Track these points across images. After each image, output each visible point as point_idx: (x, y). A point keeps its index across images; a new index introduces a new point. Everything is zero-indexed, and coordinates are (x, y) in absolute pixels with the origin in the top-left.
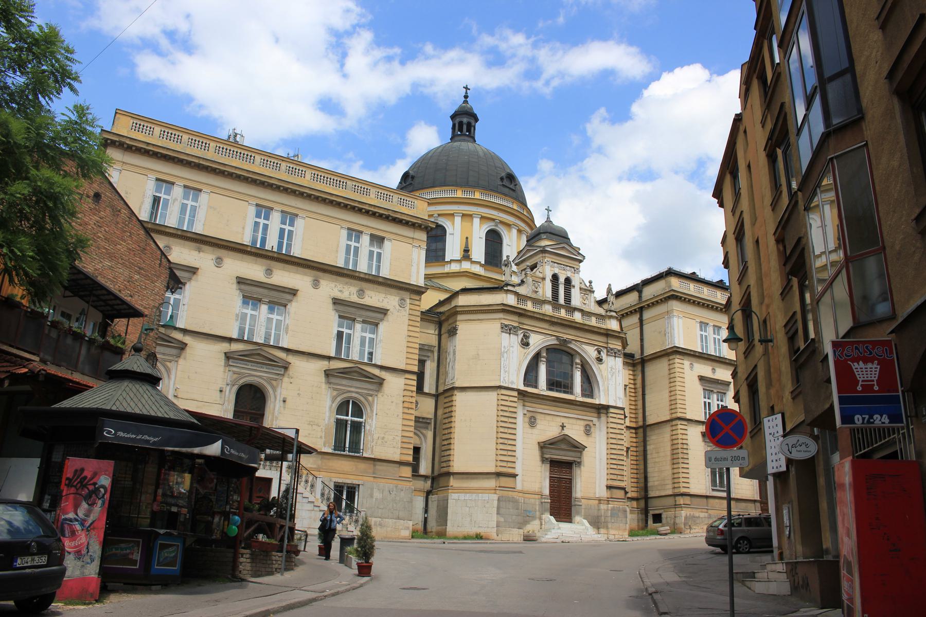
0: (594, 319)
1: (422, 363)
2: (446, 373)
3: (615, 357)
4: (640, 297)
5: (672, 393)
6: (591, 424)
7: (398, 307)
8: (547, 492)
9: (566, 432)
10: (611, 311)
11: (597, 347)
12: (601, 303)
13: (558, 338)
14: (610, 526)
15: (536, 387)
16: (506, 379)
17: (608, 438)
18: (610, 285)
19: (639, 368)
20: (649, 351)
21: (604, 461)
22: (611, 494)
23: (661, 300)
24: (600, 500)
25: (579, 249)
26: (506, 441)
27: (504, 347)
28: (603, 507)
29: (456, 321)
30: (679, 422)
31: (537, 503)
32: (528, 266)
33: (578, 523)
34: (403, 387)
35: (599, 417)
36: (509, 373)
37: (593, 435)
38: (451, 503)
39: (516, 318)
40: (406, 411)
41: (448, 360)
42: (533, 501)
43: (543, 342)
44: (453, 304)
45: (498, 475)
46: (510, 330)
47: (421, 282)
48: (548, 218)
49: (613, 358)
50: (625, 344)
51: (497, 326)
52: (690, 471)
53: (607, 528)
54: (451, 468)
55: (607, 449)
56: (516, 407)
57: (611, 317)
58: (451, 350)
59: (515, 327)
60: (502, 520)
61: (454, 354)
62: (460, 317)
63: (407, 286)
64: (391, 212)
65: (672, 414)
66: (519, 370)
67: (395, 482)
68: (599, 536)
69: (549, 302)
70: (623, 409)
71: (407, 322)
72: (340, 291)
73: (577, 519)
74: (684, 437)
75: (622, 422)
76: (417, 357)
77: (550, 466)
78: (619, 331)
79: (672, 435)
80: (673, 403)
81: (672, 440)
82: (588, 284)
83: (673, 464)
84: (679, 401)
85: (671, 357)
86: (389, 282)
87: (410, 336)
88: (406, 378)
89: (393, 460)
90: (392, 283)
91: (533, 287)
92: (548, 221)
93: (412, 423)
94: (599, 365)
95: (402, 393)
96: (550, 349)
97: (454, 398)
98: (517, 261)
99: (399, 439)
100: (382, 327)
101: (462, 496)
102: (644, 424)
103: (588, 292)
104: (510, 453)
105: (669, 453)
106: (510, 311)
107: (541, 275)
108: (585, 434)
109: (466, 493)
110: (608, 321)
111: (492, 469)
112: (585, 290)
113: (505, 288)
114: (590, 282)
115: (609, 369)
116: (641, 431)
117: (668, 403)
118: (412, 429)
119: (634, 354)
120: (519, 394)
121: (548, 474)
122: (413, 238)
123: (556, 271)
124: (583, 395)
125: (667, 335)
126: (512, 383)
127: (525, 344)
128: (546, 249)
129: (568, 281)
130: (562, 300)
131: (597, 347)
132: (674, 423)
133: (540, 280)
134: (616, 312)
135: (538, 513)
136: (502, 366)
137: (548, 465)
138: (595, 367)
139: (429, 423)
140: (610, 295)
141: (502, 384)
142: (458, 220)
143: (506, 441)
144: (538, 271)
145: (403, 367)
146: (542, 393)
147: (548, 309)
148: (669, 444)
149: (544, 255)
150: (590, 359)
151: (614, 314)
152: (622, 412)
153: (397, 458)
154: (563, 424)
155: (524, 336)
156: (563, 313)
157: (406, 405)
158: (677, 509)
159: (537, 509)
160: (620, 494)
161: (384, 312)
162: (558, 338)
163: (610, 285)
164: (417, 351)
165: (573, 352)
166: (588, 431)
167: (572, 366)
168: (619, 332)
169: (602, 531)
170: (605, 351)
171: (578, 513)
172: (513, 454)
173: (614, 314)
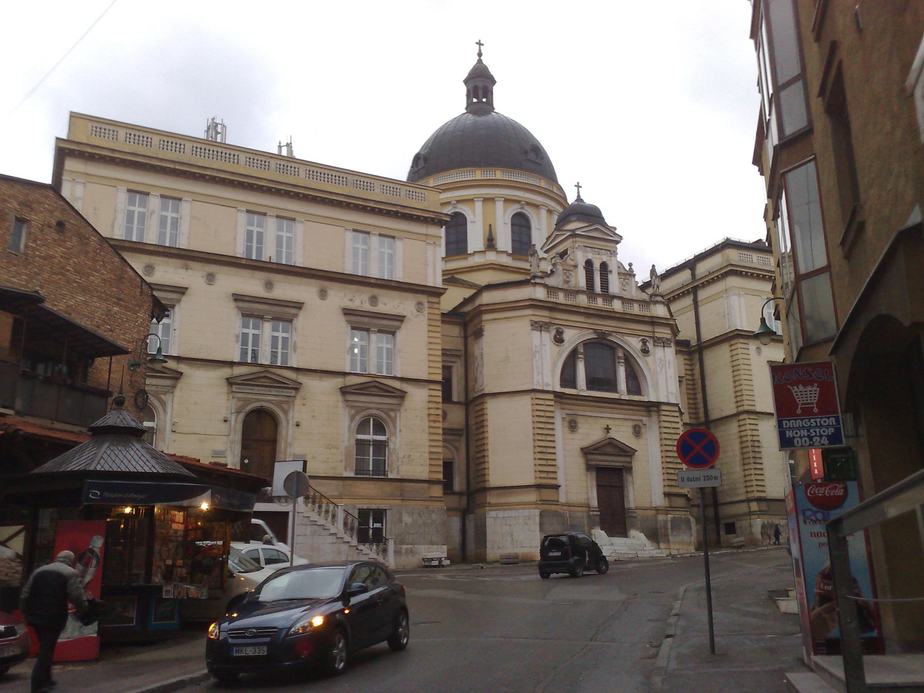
0: (636, 306)
1: (447, 369)
2: (476, 380)
3: (664, 347)
4: (693, 275)
5: (737, 383)
6: (640, 424)
7: (415, 312)
8: (594, 503)
9: (612, 434)
10: (656, 295)
11: (642, 338)
12: (645, 286)
13: (595, 331)
14: (671, 539)
15: (575, 387)
16: (540, 381)
17: (661, 439)
18: (653, 266)
19: (697, 356)
20: (706, 335)
21: (660, 466)
22: (670, 501)
23: (717, 276)
24: (657, 510)
25: (615, 228)
26: (544, 450)
27: (536, 347)
28: (661, 517)
29: (481, 322)
30: (745, 416)
32: (557, 254)
33: (634, 537)
34: (427, 399)
35: (650, 416)
36: (542, 374)
37: (644, 436)
38: (489, 522)
40: (432, 424)
41: (476, 365)
42: (580, 514)
43: (579, 337)
44: (478, 302)
45: (538, 487)
46: (541, 327)
47: (439, 283)
48: (579, 196)
50: (675, 331)
51: (526, 323)
52: (766, 472)
54: (487, 483)
55: (662, 451)
56: (553, 412)
57: (656, 302)
58: (477, 353)
59: (546, 323)
61: (482, 358)
62: (485, 317)
63: (424, 289)
64: (399, 207)
65: (738, 407)
66: (553, 370)
68: (660, 551)
69: (583, 292)
70: (677, 405)
71: (426, 327)
72: (351, 300)
73: (633, 533)
74: (754, 433)
75: (678, 420)
76: (440, 365)
77: (597, 474)
78: (669, 317)
79: (740, 432)
80: (738, 394)
81: (741, 437)
82: (627, 268)
83: (744, 464)
84: (745, 392)
85: (733, 342)
86: (404, 286)
87: (431, 343)
88: (430, 389)
90: (407, 286)
91: (565, 277)
92: (579, 199)
93: (440, 438)
94: (646, 358)
96: (587, 344)
97: (486, 406)
98: (545, 249)
99: (427, 455)
100: (400, 335)
101: (501, 514)
102: (705, 420)
103: (628, 277)
104: (550, 462)
105: (738, 452)
107: (572, 263)
109: (504, 510)
110: (652, 306)
111: (532, 481)
112: (625, 274)
113: (533, 281)
114: (630, 265)
115: (658, 362)
117: (734, 395)
118: (440, 444)
120: (555, 396)
121: (594, 483)
122: (426, 235)
123: (590, 256)
124: (629, 392)
125: (727, 316)
126: (548, 385)
127: (559, 340)
128: (577, 232)
129: (604, 266)
131: (642, 338)
132: (742, 417)
134: (662, 297)
136: (534, 367)
137: (594, 474)
138: (640, 360)
139: (460, 435)
140: (654, 277)
142: (479, 205)
143: (544, 450)
144: (569, 258)
146: (581, 393)
147: (582, 300)
148: (738, 441)
149: (574, 239)
150: (635, 352)
151: (660, 299)
152: (676, 409)
153: (425, 476)
154: (608, 426)
155: (557, 331)
156: (600, 303)
157: (432, 418)
158: (752, 517)
159: (586, 523)
160: (680, 502)
161: (400, 319)
162: (595, 331)
163: (653, 266)
165: (615, 346)
166: (637, 432)
168: (667, 319)
169: (662, 546)
170: (651, 341)
171: (633, 526)
172: (553, 463)
173: (660, 299)
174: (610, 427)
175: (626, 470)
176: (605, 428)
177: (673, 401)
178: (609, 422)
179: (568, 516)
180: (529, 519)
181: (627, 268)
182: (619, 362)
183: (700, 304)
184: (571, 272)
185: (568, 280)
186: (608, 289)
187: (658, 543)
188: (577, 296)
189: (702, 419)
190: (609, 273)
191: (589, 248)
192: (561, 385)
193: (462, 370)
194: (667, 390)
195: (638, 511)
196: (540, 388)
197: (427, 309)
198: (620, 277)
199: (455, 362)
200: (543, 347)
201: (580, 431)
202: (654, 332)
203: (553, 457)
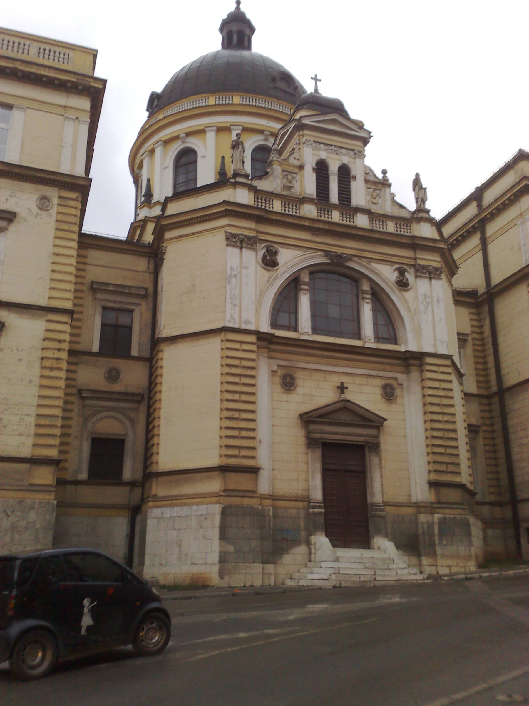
3: (430, 279)
4: (479, 206)
6: (394, 383)
7: (35, 210)
8: (317, 495)
9: (349, 396)
13: (327, 253)
14: (439, 550)
15: (296, 330)
17: (425, 405)
18: (417, 175)
19: (486, 308)
20: (497, 278)
21: (422, 441)
22: (438, 494)
24: (418, 507)
26: (236, 415)
27: (232, 269)
28: (423, 518)
31: (302, 516)
34: (42, 334)
35: (408, 372)
37: (399, 400)
39: (252, 225)
40: (47, 373)
42: (294, 512)
43: (301, 261)
49: (427, 281)
51: (221, 237)
53: (434, 555)
56: (253, 360)
59: (249, 238)
60: (230, 548)
64: (18, 63)
66: (259, 303)
67: (20, 495)
70: (449, 357)
71: (52, 233)
86: (16, 170)
87: (58, 255)
88: (48, 321)
89: (18, 456)
90: (23, 172)
91: (285, 181)
94: (404, 293)
95: (40, 344)
99: (32, 420)
101: (168, 512)
103: (380, 187)
106: (240, 213)
107: (297, 163)
108: (384, 400)
111: (214, 461)
114: (384, 172)
115: (421, 298)
116: (496, 399)
119: (477, 291)
120: (258, 339)
121: (318, 466)
122: (65, 107)
123: (323, 155)
124: (378, 338)
125: (523, 248)
126: (247, 322)
130: (334, 197)
133: (296, 170)
135: (303, 534)
136: (228, 297)
138: (396, 296)
139: (139, 402)
141: (228, 324)
142: (211, 136)
143: (236, 415)
145: (43, 302)
149: (301, 133)
150: (387, 284)
152: (448, 362)
153: (26, 452)
155: (268, 251)
156: (336, 216)
157: (47, 363)
159: (302, 525)
160: (454, 495)
162: (327, 253)
163: (417, 175)
164: (73, 279)
165: (357, 276)
167: (357, 296)
168: (434, 241)
170: (412, 271)
171: (379, 532)
172: (251, 434)
174: (345, 385)
175: (369, 448)
176: (338, 387)
177: (445, 352)
178: (346, 380)
179: (271, 513)
180: (206, 519)
181: (380, 176)
182: (363, 298)
183: (488, 241)
184: (295, 175)
185: (289, 184)
186: (350, 202)
187: (419, 556)
188: (302, 206)
189: (495, 389)
190: (352, 179)
191: (322, 146)
192: (271, 325)
193: (148, 316)
194: (435, 336)
195: (388, 508)
196: (236, 326)
197: (56, 206)
198: (368, 186)
199: (138, 304)
200: (244, 270)
201: (299, 390)
202: (416, 259)
203: (251, 425)
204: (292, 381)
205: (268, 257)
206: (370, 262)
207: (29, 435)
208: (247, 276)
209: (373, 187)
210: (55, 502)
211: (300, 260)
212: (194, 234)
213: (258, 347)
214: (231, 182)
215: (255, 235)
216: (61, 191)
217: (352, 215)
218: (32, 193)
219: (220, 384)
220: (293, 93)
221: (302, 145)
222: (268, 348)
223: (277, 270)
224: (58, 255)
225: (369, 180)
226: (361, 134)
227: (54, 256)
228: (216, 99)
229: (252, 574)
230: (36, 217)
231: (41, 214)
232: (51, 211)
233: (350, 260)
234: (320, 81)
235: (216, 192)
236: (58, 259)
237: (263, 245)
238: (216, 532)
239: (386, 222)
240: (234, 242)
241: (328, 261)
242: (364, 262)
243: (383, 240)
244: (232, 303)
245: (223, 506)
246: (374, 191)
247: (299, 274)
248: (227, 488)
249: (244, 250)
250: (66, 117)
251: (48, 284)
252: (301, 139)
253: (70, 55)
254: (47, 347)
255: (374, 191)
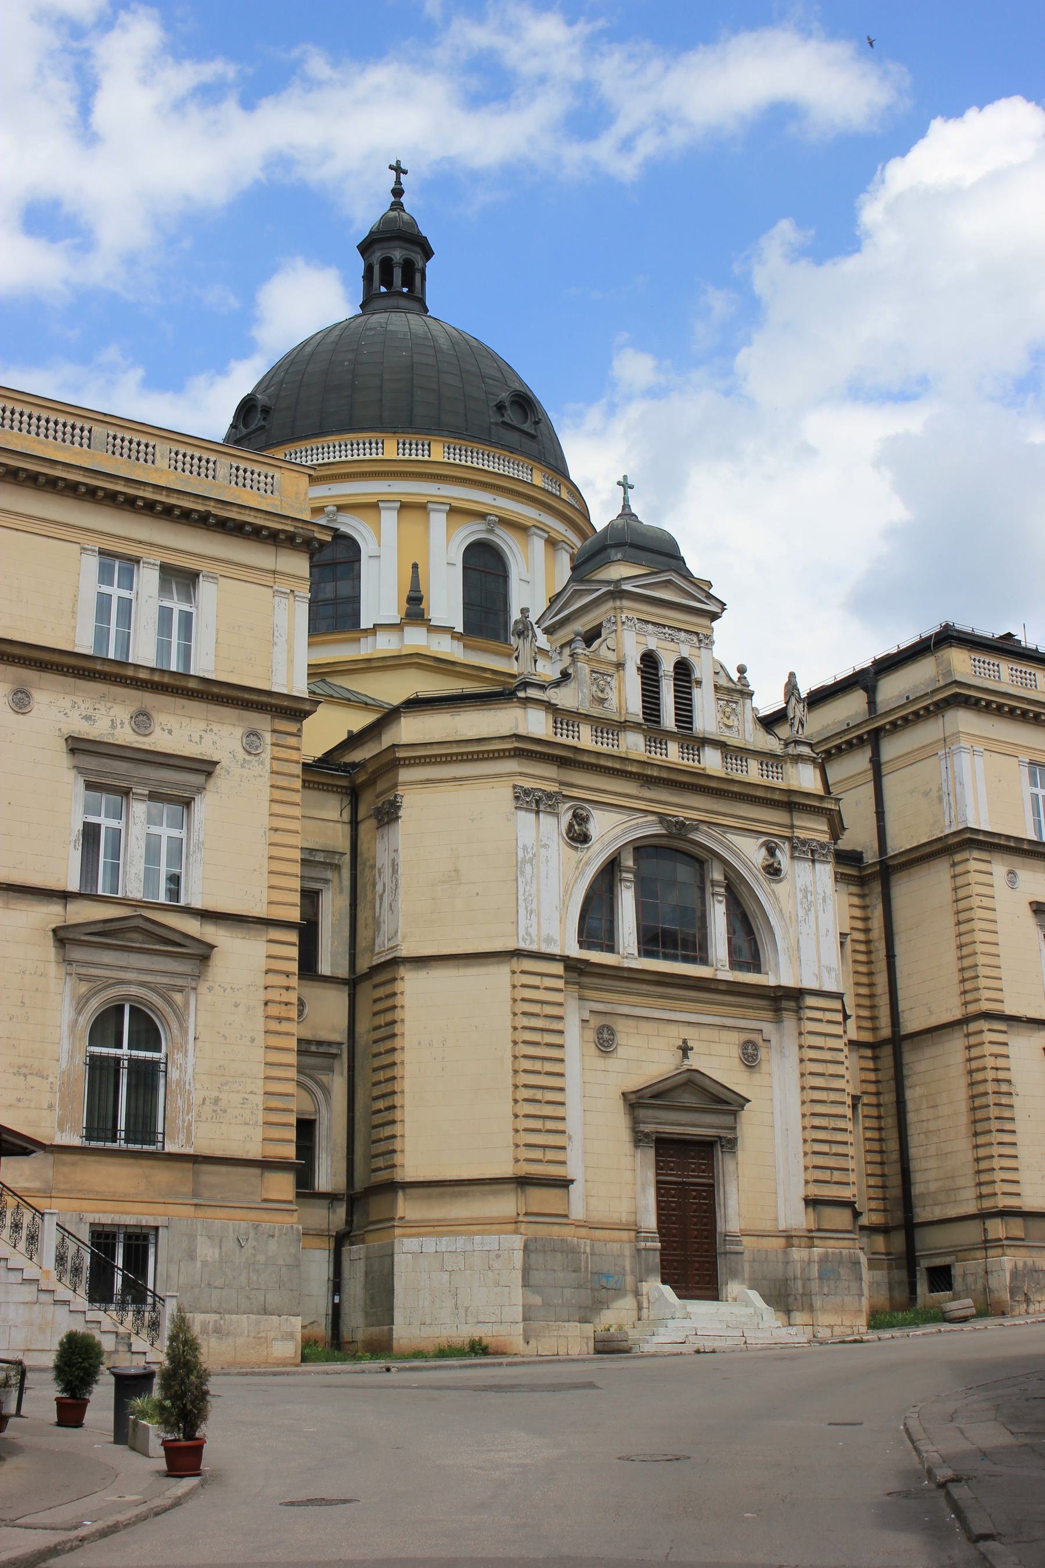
0: (753, 765)
1: (310, 897)
2: (377, 923)
3: (813, 861)
4: (872, 703)
5: (965, 951)
7: (241, 754)
8: (650, 1221)
9: (695, 1062)
10: (797, 742)
11: (764, 839)
12: (770, 722)
13: (662, 818)
14: (817, 1302)
15: (611, 948)
16: (533, 931)
17: (802, 1075)
18: (792, 675)
19: (877, 888)
20: (900, 841)
21: (797, 1134)
22: (819, 1218)
23: (926, 708)
24: (789, 1237)
25: (710, 584)
26: (539, 1095)
27: (525, 848)
28: (798, 1254)
29: (395, 785)
30: (984, 1025)
31: (627, 1252)
32: (577, 634)
33: (735, 1300)
34: (263, 964)
35: (778, 1021)
36: (538, 916)
37: (764, 1066)
38: (402, 1264)
39: (550, 771)
40: (274, 1026)
41: (379, 888)
42: (616, 1247)
43: (624, 833)
44: (388, 739)
45: (523, 1182)
46: (537, 802)
47: (300, 687)
48: (626, 506)
49: (808, 865)
50: (837, 828)
51: (504, 793)
52: (1021, 1151)
53: (811, 1309)
54: (399, 1170)
55: (803, 1102)
56: (561, 1005)
57: (798, 758)
58: (383, 859)
59: (550, 796)
60: (537, 1300)
61: (395, 871)
62: (405, 775)
63: (264, 699)
64: (212, 504)
65: (965, 1004)
66: (565, 907)
67: (253, 1215)
68: (793, 1330)
69: (636, 726)
71: (266, 793)
72: (88, 718)
73: (733, 1288)
74: (1001, 1063)
75: (838, 1030)
76: (296, 884)
77: (657, 1155)
78: (822, 793)
79: (970, 1060)
80: (968, 975)
81: (970, 1072)
82: (735, 676)
83: (976, 1134)
84: (982, 971)
85: (958, 857)
87: (276, 830)
89: (245, 1156)
90: (223, 691)
91: (594, 688)
92: (626, 512)
93: (292, 1058)
94: (773, 885)
95: (261, 980)
96: (642, 849)
97: (399, 986)
98: (547, 623)
99: (259, 1100)
100: (201, 807)
101: (430, 1244)
102: (893, 1032)
103: (736, 697)
104: (550, 1125)
105: (963, 1106)
106: (537, 752)
107: (612, 657)
108: (743, 1068)
109: (441, 1235)
110: (789, 768)
111: (506, 1169)
112: (729, 691)
113: (521, 694)
114: (742, 670)
115: (800, 895)
116: (887, 1051)
117: (956, 977)
118: (292, 1073)
119: (861, 853)
120: (567, 968)
121: (651, 1175)
122: (274, 572)
123: (653, 643)
124: (735, 964)
125: (945, 799)
126: (549, 940)
127: (578, 837)
128: (624, 587)
129: (683, 669)
130: (669, 720)
131: (764, 839)
132: (973, 1027)
133: (611, 670)
134: (810, 745)
135: (629, 1279)
136: (521, 898)
137: (651, 1153)
138: (762, 889)
139: (335, 1056)
140: (793, 701)
141: (522, 945)
142: (389, 518)
143: (539, 1095)
144: (604, 646)
145: (260, 910)
147: (633, 745)
148: (963, 1081)
149: (618, 603)
150: (750, 869)
151: (805, 750)
152: (836, 1005)
153: (254, 1150)
154: (685, 1041)
155: (575, 816)
156: (673, 753)
157: (274, 1010)
158: (991, 1252)
159: (628, 1267)
160: (840, 1218)
161: (206, 768)
162: (662, 818)
163: (792, 675)
164: (297, 869)
166: (750, 1057)
167: (702, 890)
168: (821, 798)
170: (786, 847)
171: (734, 1274)
173: (805, 750)
174: (690, 1044)
175: (722, 1146)
176: (680, 1048)
177: (830, 985)
178: (687, 1033)
179: (588, 1250)
180: (498, 1256)
181: (735, 676)
182: (713, 894)
183: (885, 770)
184: (609, 679)
185: (601, 695)
186: (691, 723)
187: (788, 1312)
188: (622, 735)
189: (886, 1032)
190: (694, 684)
191: (650, 627)
192: (579, 942)
193: (345, 901)
194: (819, 961)
195: (745, 1240)
196: (534, 948)
197: (269, 747)
198: (719, 696)
199: (326, 881)
200: (543, 851)
201: (621, 1052)
202: (792, 827)
203: (558, 1111)
204: (612, 1037)
205: (576, 827)
206: (725, 832)
207: (256, 1123)
208: (548, 861)
209: (726, 697)
210: (300, 1227)
211: (623, 830)
212: (455, 779)
213: (566, 983)
214: (520, 698)
215: (557, 789)
216: (276, 720)
217: (696, 748)
218: (234, 725)
219: (511, 1045)
220: (533, 432)
221: (620, 626)
222: (578, 984)
223: (588, 848)
224: (276, 830)
225: (721, 686)
226: (713, 608)
227: (272, 832)
228: (398, 444)
229: (567, 1337)
230: (242, 766)
231: (250, 762)
232: (263, 755)
233: (697, 829)
234: (631, 487)
235: (490, 709)
236: (278, 838)
237: (568, 805)
238: (518, 1275)
239: (746, 762)
240: (527, 802)
241: (664, 832)
242: (715, 832)
243: (744, 795)
244: (526, 908)
245: (525, 1237)
246: (727, 705)
247: (619, 854)
248: (529, 1211)
249: (541, 815)
250: (277, 591)
251: (265, 880)
252: (618, 615)
253: (275, 478)
254: (271, 984)
255: (727, 705)
